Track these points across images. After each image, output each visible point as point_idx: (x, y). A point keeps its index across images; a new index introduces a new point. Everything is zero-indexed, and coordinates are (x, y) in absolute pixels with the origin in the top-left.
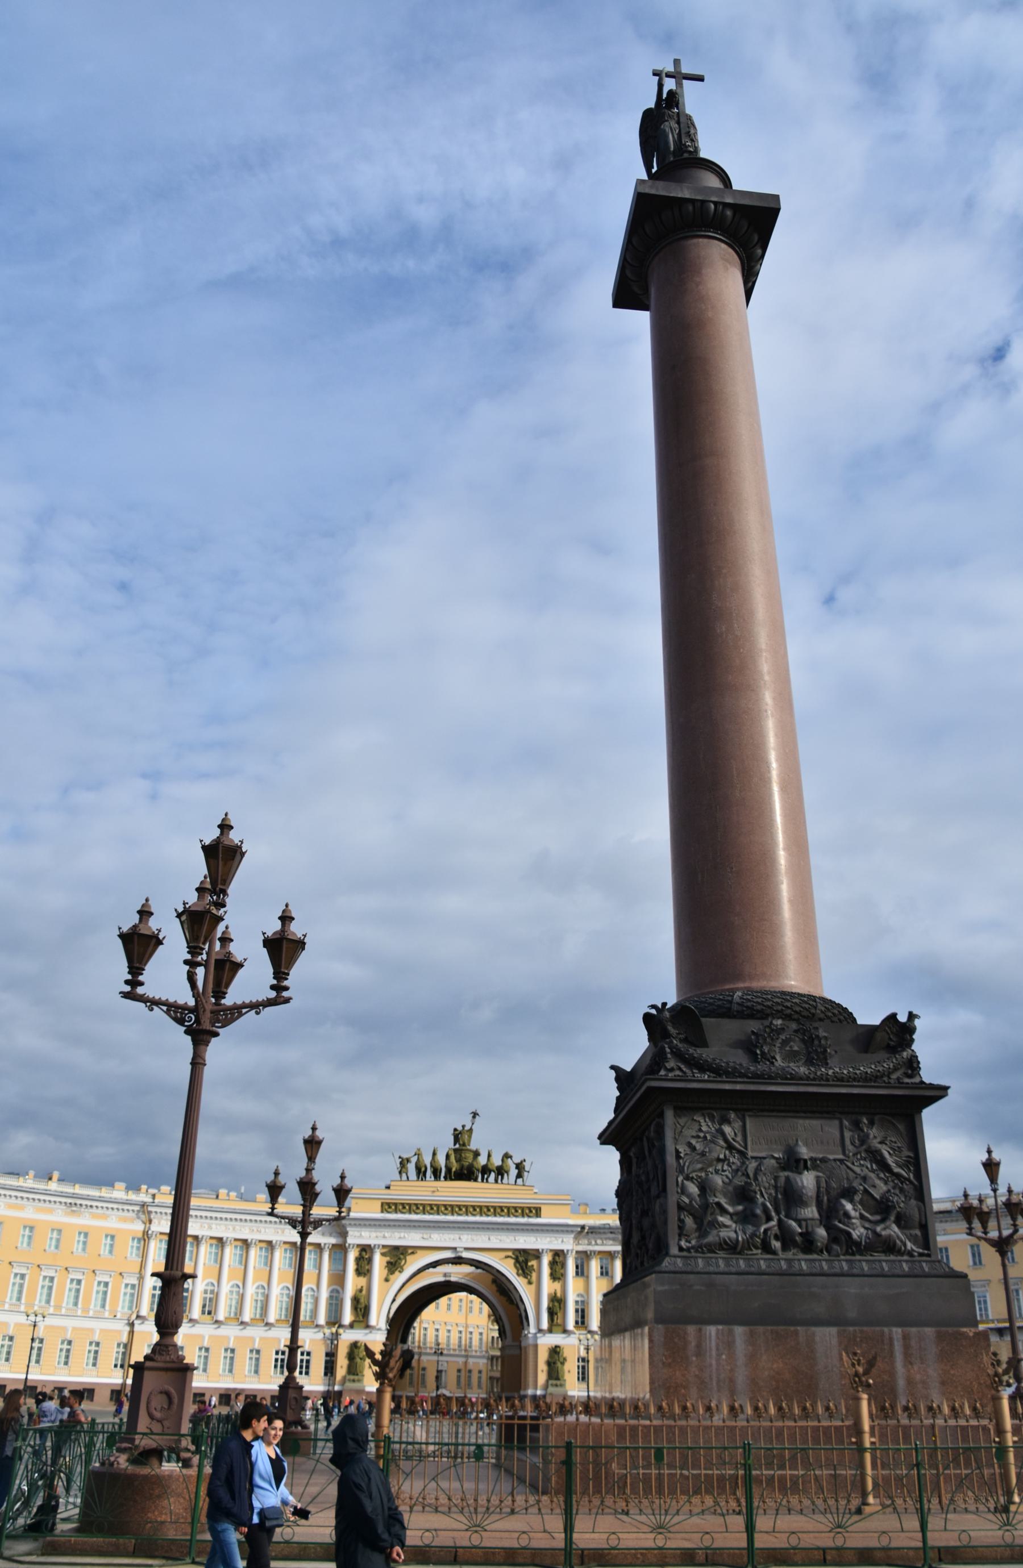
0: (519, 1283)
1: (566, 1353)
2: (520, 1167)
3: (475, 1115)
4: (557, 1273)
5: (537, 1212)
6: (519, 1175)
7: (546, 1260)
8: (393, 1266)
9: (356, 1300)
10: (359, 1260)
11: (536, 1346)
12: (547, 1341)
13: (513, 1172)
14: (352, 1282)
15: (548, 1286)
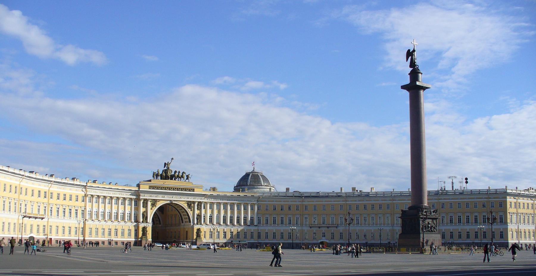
0: (189, 210)
1: (201, 230)
2: (188, 176)
3: (172, 159)
4: (199, 208)
5: (193, 190)
6: (187, 179)
7: (196, 204)
8: (153, 205)
9: (143, 214)
10: (143, 203)
11: (193, 228)
12: (196, 227)
13: (185, 178)
14: (142, 210)
15: (197, 212)
